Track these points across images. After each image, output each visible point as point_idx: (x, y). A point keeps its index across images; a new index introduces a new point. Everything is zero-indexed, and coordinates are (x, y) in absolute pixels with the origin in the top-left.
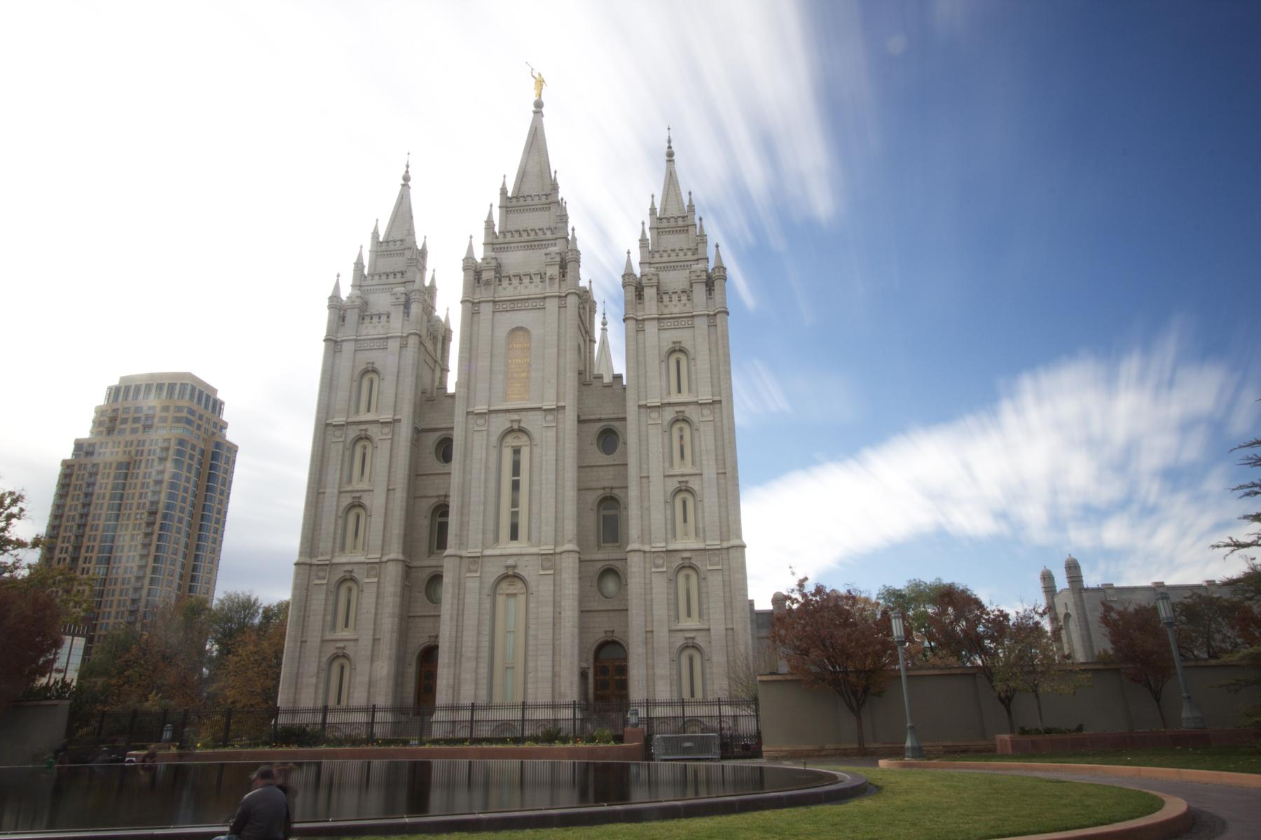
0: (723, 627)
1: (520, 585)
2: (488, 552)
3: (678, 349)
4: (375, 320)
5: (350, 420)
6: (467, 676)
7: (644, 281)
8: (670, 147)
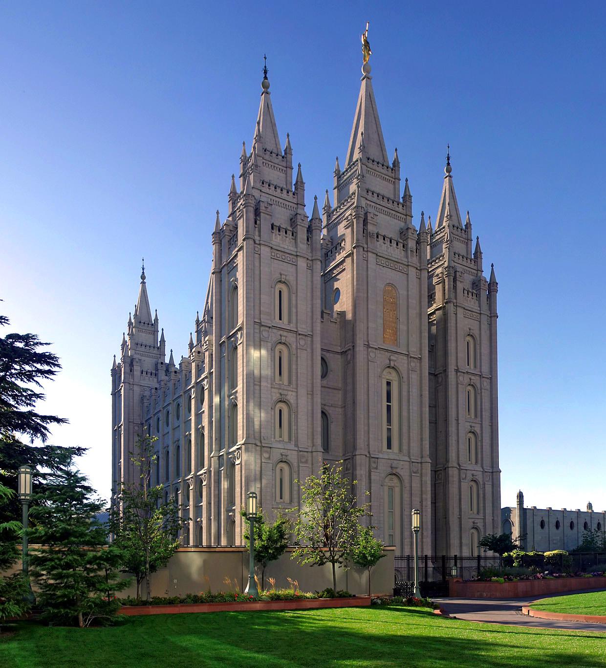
2: (381, 456)
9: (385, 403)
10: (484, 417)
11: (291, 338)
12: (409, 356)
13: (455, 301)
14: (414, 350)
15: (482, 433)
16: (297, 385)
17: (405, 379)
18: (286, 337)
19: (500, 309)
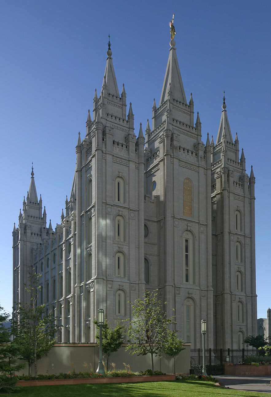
2: (182, 286)
9: (184, 253)
10: (246, 262)
11: (125, 213)
12: (200, 224)
13: (228, 189)
14: (202, 220)
15: (245, 272)
16: (129, 242)
17: (197, 238)
18: (122, 211)
19: (256, 195)
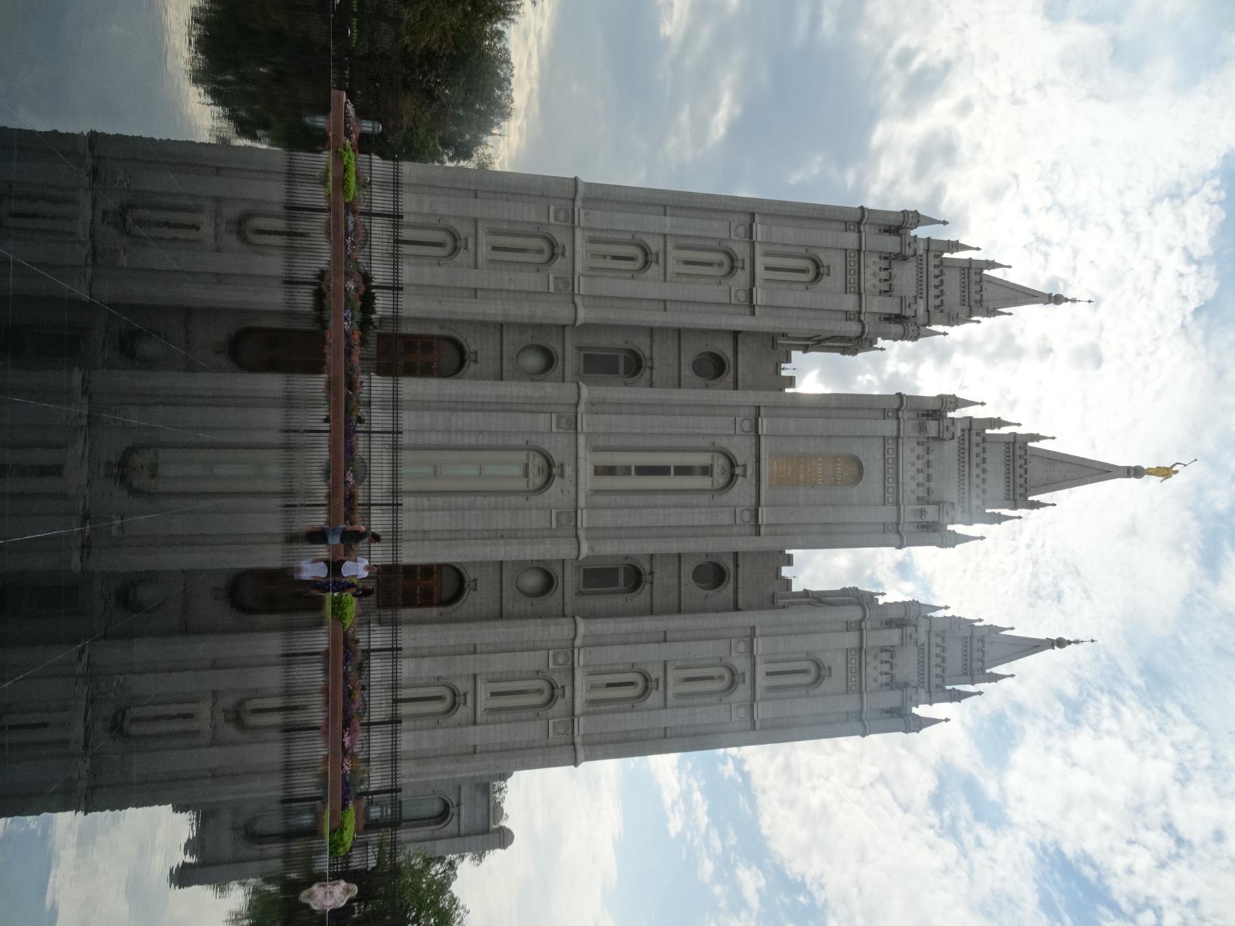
0: (478, 742)
1: (538, 481)
2: (582, 440)
3: (821, 672)
4: (884, 275)
5: (757, 246)
6: (427, 418)
7: (910, 630)
8: (1069, 643)
